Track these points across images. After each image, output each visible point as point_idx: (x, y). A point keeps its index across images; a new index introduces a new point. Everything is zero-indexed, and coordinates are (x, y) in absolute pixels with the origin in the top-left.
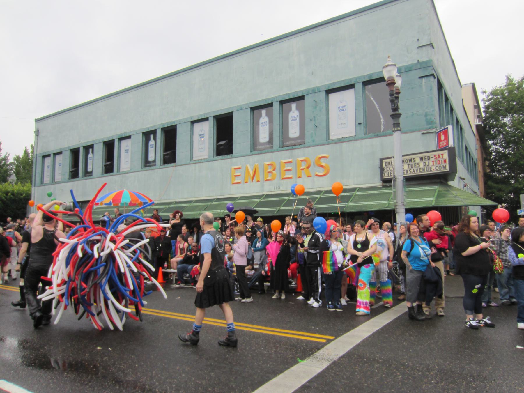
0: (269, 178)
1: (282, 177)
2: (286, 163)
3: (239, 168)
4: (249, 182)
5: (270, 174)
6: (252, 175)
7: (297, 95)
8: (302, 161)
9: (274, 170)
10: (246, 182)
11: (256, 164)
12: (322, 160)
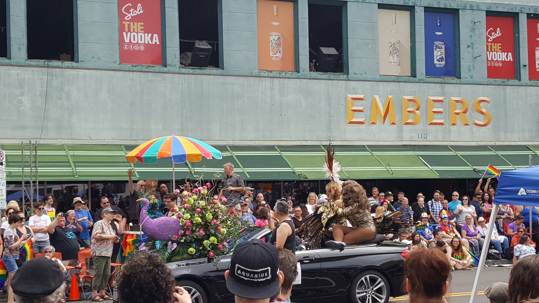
0: (409, 121)
2: (434, 101)
3: (361, 99)
4: (378, 123)
6: (383, 114)
7: (450, 5)
8: (457, 101)
9: (418, 109)
10: (373, 123)
12: (482, 104)
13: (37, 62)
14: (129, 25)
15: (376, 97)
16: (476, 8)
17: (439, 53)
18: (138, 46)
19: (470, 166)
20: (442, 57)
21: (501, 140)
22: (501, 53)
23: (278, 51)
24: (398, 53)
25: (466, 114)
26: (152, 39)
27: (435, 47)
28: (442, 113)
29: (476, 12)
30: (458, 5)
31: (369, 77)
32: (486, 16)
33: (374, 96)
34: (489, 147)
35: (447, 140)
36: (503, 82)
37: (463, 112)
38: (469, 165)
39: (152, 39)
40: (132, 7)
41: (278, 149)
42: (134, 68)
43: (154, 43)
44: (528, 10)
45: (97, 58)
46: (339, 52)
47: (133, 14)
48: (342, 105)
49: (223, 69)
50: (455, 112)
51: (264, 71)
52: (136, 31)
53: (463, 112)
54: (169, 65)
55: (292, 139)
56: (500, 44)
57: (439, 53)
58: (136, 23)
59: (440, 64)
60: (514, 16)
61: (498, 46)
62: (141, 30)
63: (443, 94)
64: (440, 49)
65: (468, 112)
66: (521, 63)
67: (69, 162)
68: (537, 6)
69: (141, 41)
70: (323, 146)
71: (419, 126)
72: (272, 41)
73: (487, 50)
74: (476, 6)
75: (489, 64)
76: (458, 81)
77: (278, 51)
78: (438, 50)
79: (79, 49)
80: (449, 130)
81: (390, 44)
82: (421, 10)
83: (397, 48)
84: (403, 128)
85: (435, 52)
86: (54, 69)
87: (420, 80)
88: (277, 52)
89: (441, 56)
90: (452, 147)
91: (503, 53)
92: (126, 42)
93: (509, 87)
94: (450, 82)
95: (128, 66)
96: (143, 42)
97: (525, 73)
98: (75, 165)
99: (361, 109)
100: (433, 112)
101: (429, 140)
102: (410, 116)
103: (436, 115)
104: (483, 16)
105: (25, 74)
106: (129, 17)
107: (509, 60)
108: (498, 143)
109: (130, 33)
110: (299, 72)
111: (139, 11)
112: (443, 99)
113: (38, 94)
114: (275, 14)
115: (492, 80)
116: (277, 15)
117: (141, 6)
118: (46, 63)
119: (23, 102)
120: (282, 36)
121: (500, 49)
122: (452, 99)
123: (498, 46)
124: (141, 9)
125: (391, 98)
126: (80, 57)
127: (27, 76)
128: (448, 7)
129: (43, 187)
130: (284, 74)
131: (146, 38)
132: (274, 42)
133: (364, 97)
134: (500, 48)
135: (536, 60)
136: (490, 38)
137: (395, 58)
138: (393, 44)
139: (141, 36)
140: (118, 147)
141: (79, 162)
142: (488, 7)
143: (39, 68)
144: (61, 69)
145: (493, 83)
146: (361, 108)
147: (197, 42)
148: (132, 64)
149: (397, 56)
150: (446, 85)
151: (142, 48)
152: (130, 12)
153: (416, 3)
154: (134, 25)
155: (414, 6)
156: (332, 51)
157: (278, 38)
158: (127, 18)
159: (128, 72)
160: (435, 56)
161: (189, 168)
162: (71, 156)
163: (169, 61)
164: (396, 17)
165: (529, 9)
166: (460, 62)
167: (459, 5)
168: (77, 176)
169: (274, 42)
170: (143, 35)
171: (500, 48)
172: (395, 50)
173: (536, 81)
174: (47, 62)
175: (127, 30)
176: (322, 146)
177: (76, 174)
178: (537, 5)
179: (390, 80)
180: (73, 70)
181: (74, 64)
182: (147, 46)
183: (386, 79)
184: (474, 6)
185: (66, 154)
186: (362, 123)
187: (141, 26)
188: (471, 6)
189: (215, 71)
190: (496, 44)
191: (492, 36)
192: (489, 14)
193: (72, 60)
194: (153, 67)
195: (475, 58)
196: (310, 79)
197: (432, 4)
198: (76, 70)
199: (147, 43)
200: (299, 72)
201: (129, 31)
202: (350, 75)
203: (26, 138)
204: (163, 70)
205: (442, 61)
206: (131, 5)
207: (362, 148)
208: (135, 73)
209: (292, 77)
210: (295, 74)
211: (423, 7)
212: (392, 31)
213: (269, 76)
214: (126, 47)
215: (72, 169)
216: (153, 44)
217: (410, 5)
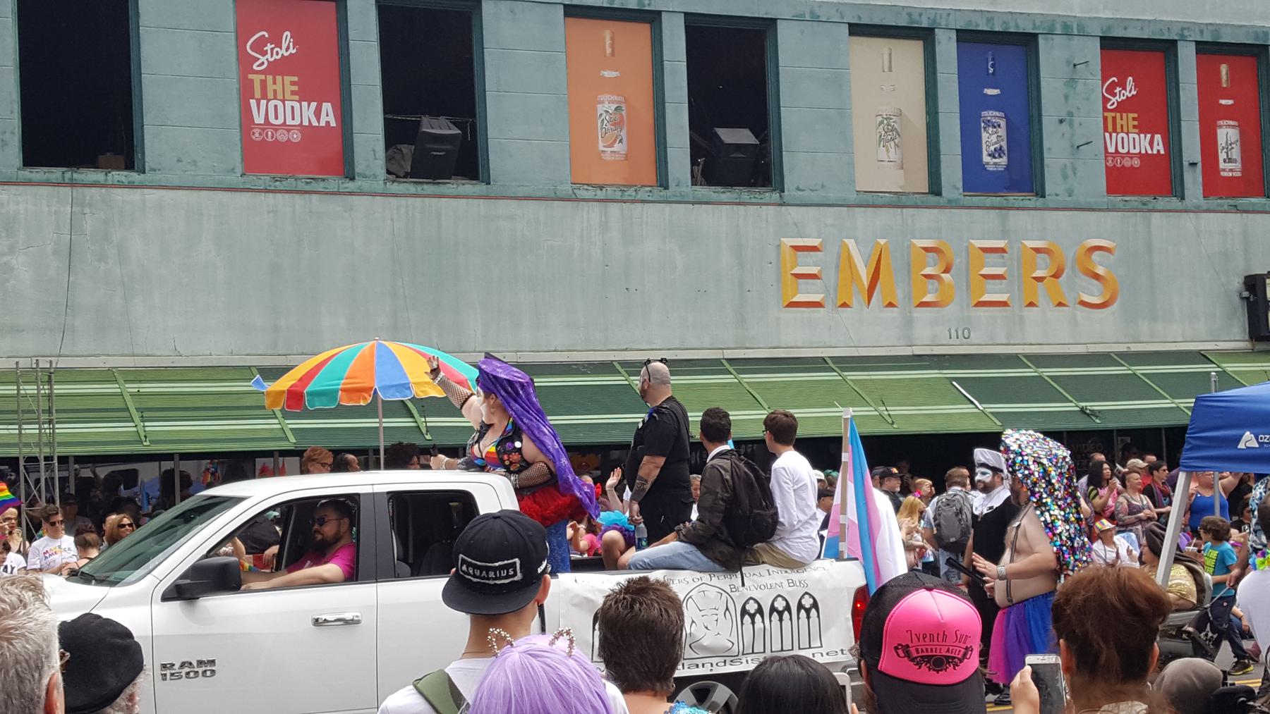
0: (928, 298)
1: (974, 303)
3: (814, 249)
5: (935, 283)
6: (866, 284)
7: (1017, 26)
8: (1037, 250)
9: (947, 271)
10: (844, 305)
11: (882, 242)
12: (1096, 256)
13: (45, 173)
14: (264, 83)
15: (850, 246)
16: (1078, 30)
17: (994, 138)
18: (285, 132)
19: (1071, 402)
20: (1001, 147)
21: (1142, 339)
22: (1136, 136)
23: (617, 137)
24: (898, 139)
25: (1061, 279)
26: (318, 113)
27: (983, 124)
28: (1005, 278)
29: (1076, 41)
30: (1034, 24)
31: (832, 196)
32: (1102, 48)
33: (844, 240)
34: (1116, 357)
35: (1016, 342)
36: (1144, 204)
37: (1052, 276)
38: (1070, 398)
39: (318, 113)
40: (270, 40)
41: (622, 370)
42: (277, 183)
43: (323, 124)
44: (1198, 32)
45: (189, 163)
46: (761, 137)
47: (272, 57)
48: (771, 263)
49: (488, 183)
50: (1034, 275)
51: (586, 187)
52: (280, 96)
53: (1052, 276)
54: (360, 175)
55: (654, 347)
56: (1136, 115)
57: (992, 138)
58: (279, 78)
59: (995, 164)
60: (1165, 48)
61: (1130, 119)
62: (293, 93)
63: (1004, 234)
64: (995, 127)
65: (1064, 275)
66: (1184, 159)
67: (127, 409)
68: (1219, 24)
69: (293, 119)
70: (728, 360)
71: (951, 311)
72: (601, 115)
73: (1106, 130)
74: (1078, 25)
75: (1110, 162)
76: (1040, 202)
77: (617, 137)
78: (990, 130)
79: (146, 141)
80: (1021, 318)
81: (880, 119)
82: (950, 38)
83: (896, 126)
84: (915, 315)
85: (984, 136)
86: (87, 190)
87: (950, 201)
88: (615, 141)
89: (997, 146)
90: (1029, 357)
91: (1142, 136)
92: (256, 122)
93: (1158, 213)
94: (1021, 204)
95: (264, 180)
96: (297, 122)
97: (1193, 181)
98: (142, 417)
99: (816, 272)
100: (982, 275)
101: (976, 341)
102: (930, 287)
103: (991, 284)
104: (1092, 51)
105: (18, 203)
106: (263, 63)
107: (1155, 152)
108: (1136, 348)
109: (265, 101)
110: (666, 188)
111: (288, 49)
112: (1006, 245)
113: (49, 248)
114: (609, 51)
115: (1118, 199)
116: (613, 54)
117: (291, 38)
118: (68, 175)
119: (14, 268)
120: (625, 103)
121: (1134, 127)
122: (1026, 246)
123: (1129, 118)
124: (291, 44)
125: (886, 243)
126: (147, 159)
127: (22, 207)
128: (1012, 30)
129: (65, 474)
130: (631, 192)
131: (305, 113)
132: (607, 118)
133: (821, 243)
134: (1136, 123)
135: (1220, 151)
136: (1110, 100)
137: (892, 150)
138: (886, 119)
139: (293, 107)
140: (243, 372)
141: (152, 409)
142: (1105, 29)
143: (51, 188)
144: (104, 190)
145: (1121, 205)
146: (814, 270)
147: (425, 120)
148: (274, 175)
149: (897, 146)
150: (1011, 212)
151: (296, 137)
152: (266, 53)
153: (938, 21)
154: (274, 83)
155: (933, 29)
156: (744, 136)
157: (616, 109)
158: (258, 66)
159: (263, 194)
160: (984, 146)
161: (413, 417)
162: (132, 395)
163: (360, 166)
164: (890, 55)
165: (1202, 32)
166: (1042, 160)
167: (1038, 23)
168: (148, 443)
169: (607, 118)
170: (297, 105)
171: (1136, 123)
172: (891, 131)
173: (1219, 201)
174: (70, 173)
175: (258, 94)
176: (724, 362)
177: (146, 437)
178: (1218, 22)
179: (881, 202)
180: (131, 190)
181: (134, 177)
182: (307, 130)
183: (871, 201)
184: (1072, 27)
185: (119, 390)
186: (817, 305)
187: (293, 83)
188: (1066, 26)
189: (468, 187)
190: (1124, 115)
191: (1115, 94)
192: (1108, 43)
193: (129, 165)
194: (323, 180)
195: (1078, 147)
196: (693, 203)
197: (974, 24)
198: (139, 190)
199: (307, 124)
200: (666, 188)
201: (264, 96)
202: (786, 192)
203: (24, 355)
204: (347, 188)
205: (1000, 156)
206: (267, 36)
207: (818, 364)
208: (279, 195)
209: (650, 199)
210: (659, 193)
211: (955, 31)
212: (882, 88)
213: (597, 197)
214: (257, 135)
215: (136, 426)
216: (322, 127)
217: (923, 26)
